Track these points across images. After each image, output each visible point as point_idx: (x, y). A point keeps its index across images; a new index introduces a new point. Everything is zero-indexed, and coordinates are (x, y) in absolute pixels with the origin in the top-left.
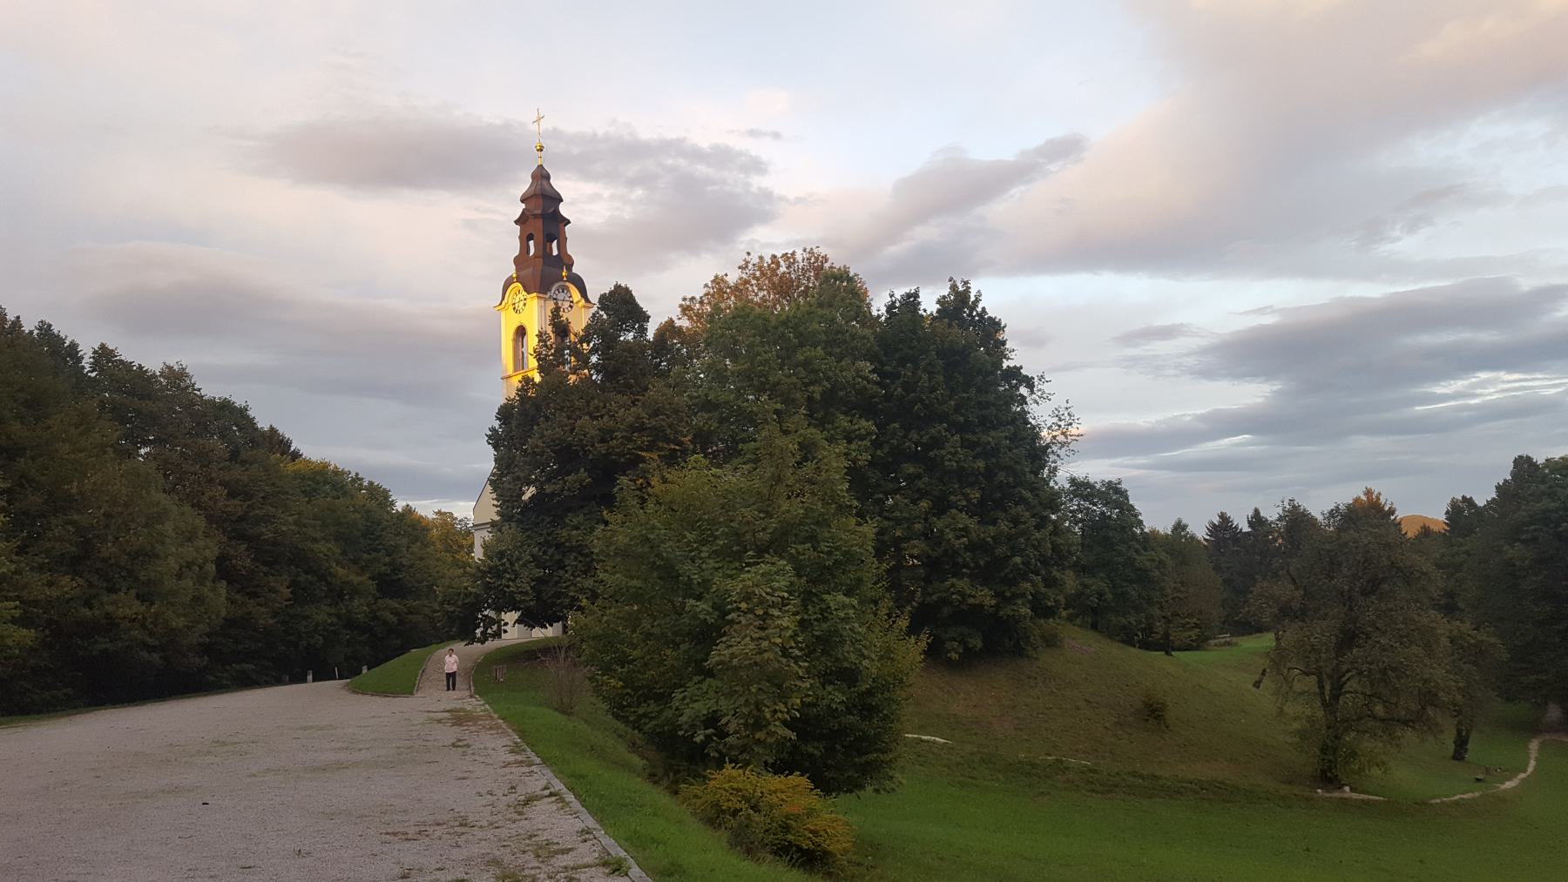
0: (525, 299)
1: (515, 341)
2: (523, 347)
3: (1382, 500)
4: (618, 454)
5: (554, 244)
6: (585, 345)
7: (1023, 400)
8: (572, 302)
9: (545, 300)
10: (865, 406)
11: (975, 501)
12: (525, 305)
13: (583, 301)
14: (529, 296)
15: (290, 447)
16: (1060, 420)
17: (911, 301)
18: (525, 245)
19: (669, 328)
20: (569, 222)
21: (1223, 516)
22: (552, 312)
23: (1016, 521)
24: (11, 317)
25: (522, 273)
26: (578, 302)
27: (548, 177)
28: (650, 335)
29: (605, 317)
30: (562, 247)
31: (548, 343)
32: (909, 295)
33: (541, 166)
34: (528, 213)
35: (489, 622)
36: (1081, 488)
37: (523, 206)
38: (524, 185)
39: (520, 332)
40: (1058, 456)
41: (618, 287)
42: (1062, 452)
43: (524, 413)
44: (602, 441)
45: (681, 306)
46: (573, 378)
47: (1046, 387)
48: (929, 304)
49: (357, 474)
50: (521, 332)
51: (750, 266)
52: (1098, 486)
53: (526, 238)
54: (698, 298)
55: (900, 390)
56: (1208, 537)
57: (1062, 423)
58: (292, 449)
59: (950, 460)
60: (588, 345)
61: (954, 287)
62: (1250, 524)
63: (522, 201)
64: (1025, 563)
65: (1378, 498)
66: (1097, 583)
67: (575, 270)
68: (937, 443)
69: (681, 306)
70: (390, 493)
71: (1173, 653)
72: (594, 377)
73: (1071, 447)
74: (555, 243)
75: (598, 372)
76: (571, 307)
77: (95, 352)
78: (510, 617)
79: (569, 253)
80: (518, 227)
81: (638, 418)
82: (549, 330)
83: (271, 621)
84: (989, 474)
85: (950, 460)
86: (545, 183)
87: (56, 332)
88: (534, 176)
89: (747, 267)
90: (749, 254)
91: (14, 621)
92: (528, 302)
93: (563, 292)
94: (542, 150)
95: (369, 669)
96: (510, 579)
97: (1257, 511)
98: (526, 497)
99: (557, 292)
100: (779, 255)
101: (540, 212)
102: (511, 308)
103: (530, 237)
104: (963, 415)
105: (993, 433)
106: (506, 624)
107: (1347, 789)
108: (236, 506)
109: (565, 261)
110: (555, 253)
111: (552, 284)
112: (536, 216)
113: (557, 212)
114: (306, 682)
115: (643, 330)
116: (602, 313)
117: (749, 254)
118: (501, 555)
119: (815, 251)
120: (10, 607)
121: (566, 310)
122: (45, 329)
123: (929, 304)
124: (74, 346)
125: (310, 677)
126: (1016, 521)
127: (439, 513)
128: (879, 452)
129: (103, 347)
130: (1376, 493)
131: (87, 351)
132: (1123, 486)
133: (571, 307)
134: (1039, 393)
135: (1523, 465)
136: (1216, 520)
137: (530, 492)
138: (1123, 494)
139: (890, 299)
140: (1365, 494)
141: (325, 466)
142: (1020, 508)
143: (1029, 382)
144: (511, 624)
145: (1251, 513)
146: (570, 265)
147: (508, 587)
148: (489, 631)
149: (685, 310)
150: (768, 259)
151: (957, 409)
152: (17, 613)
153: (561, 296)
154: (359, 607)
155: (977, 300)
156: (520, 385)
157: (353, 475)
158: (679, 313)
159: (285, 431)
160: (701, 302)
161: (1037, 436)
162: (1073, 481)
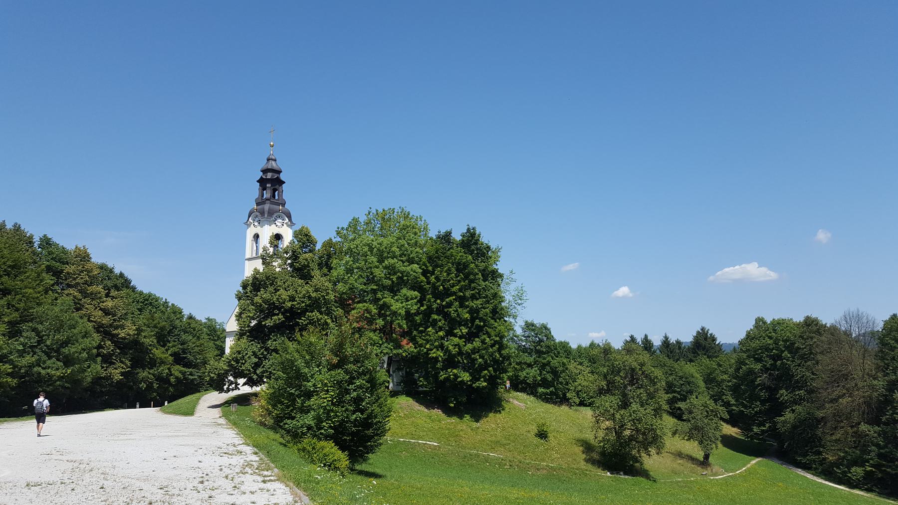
0: (260, 221)
3: (710, 332)
4: (296, 308)
6: (285, 255)
7: (499, 285)
8: (283, 223)
9: (270, 221)
10: (416, 286)
15: (130, 283)
16: (518, 293)
17: (448, 235)
18: (261, 194)
19: (329, 244)
20: (285, 183)
21: (632, 337)
22: (270, 237)
23: (483, 342)
24: (9, 226)
25: (259, 207)
26: (286, 223)
29: (297, 243)
30: (280, 195)
31: (268, 252)
34: (264, 177)
35: (231, 383)
36: (529, 326)
37: (262, 173)
38: (263, 164)
39: (256, 236)
40: (518, 310)
42: (519, 307)
43: (253, 284)
44: (290, 301)
45: (337, 231)
46: (278, 270)
48: (457, 236)
49: (166, 300)
50: (256, 237)
51: (371, 214)
54: (345, 228)
55: (433, 279)
57: (519, 294)
58: (132, 284)
59: (454, 313)
60: (287, 255)
61: (468, 229)
62: (643, 343)
64: (486, 362)
65: (708, 332)
66: (532, 374)
67: (286, 206)
68: (449, 305)
69: (337, 231)
70: (183, 311)
72: (289, 269)
73: (523, 305)
74: (277, 192)
75: (291, 267)
77: (41, 239)
78: (241, 381)
79: (284, 198)
80: (259, 184)
81: (308, 292)
82: (268, 245)
83: (121, 377)
84: (473, 320)
85: (454, 313)
86: (273, 162)
87: (22, 228)
88: (268, 160)
89: (369, 214)
90: (370, 208)
91: (8, 374)
92: (261, 222)
95: (168, 403)
96: (242, 363)
97: (646, 335)
98: (252, 325)
99: (276, 218)
100: (386, 209)
101: (270, 177)
102: (252, 225)
103: (264, 189)
104: (463, 293)
105: (475, 302)
106: (239, 384)
107: (622, 473)
108: (106, 320)
110: (277, 198)
112: (268, 180)
113: (278, 178)
114: (135, 407)
116: (295, 240)
117: (370, 208)
118: (239, 352)
119: (404, 209)
120: (8, 368)
122: (17, 228)
123: (457, 236)
124: (31, 237)
125: (138, 406)
126: (483, 342)
127: (208, 319)
128: (422, 308)
129: (45, 236)
130: (707, 329)
131: (36, 240)
132: (549, 326)
133: (283, 225)
134: (510, 279)
135: (760, 322)
136: (628, 339)
137: (253, 323)
138: (549, 330)
139: (438, 234)
140: (702, 330)
141: (150, 295)
142: (485, 336)
143: (501, 276)
144: (241, 385)
145: (643, 337)
146: (283, 205)
147: (241, 367)
148: (230, 387)
149: (338, 233)
150: (380, 210)
151: (460, 290)
152: (10, 371)
154: (164, 370)
155: (479, 236)
156: (253, 273)
157: (164, 300)
158: (335, 233)
159: (128, 274)
160: (347, 229)
161: (502, 300)
162: (526, 322)
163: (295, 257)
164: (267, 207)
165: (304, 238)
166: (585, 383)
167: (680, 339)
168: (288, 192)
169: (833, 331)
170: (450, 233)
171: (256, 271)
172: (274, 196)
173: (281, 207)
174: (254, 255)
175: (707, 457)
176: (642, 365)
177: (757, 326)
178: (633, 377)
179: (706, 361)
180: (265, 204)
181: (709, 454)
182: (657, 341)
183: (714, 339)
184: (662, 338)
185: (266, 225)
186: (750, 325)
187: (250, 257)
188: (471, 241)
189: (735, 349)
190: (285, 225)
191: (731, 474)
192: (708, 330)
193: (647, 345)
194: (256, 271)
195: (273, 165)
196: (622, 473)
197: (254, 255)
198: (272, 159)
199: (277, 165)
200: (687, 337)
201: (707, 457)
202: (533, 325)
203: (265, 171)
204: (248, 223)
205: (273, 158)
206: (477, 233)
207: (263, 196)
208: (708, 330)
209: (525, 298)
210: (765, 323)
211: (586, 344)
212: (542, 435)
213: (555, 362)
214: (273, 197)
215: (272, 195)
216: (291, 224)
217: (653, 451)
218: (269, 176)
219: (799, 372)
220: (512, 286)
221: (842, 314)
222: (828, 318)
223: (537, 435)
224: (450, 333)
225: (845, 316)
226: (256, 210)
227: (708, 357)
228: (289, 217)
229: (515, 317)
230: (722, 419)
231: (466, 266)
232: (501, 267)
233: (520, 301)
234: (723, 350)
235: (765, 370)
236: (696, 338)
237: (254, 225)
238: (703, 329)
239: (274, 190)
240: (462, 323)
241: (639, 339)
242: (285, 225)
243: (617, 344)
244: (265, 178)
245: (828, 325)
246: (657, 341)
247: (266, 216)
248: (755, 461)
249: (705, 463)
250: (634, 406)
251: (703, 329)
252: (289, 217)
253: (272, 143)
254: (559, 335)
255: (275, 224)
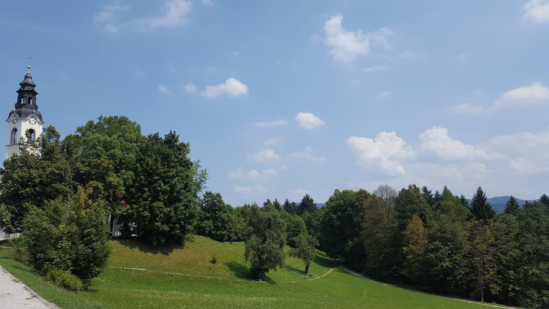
0: (18, 119)
1: (12, 133)
2: (15, 135)
3: (310, 198)
5: (31, 101)
8: (36, 121)
9: (25, 120)
11: (166, 199)
12: (17, 121)
13: (40, 122)
14: (19, 119)
20: (37, 94)
21: (268, 200)
27: (31, 78)
28: (61, 139)
32: (156, 134)
33: (29, 74)
34: (22, 89)
36: (208, 194)
37: (21, 86)
38: (22, 80)
39: (15, 129)
41: (51, 126)
47: (200, 164)
48: (162, 136)
52: (214, 194)
53: (20, 98)
56: (263, 206)
61: (171, 132)
63: (20, 85)
65: (309, 197)
67: (38, 110)
68: (156, 181)
71: (233, 243)
76: (35, 123)
79: (36, 104)
80: (18, 93)
86: (30, 80)
88: (26, 77)
93: (33, 118)
94: (30, 68)
97: (276, 199)
99: (30, 118)
102: (12, 121)
103: (23, 97)
107: (261, 280)
109: (36, 108)
110: (31, 104)
111: (29, 115)
115: (58, 138)
121: (33, 124)
123: (162, 136)
130: (309, 195)
135: (336, 190)
136: (266, 201)
140: (306, 196)
153: (32, 119)
163: (44, 144)
164: (23, 110)
165: (51, 132)
166: (241, 227)
167: (294, 201)
168: (39, 100)
169: (374, 196)
170: (158, 134)
171: (14, 155)
172: (29, 103)
173: (34, 111)
174: (13, 144)
175: (307, 268)
176: (275, 217)
177: (335, 194)
178: (269, 224)
179: (307, 214)
180: (22, 108)
181: (308, 267)
182: (282, 203)
183: (312, 201)
184: (285, 201)
185: (23, 122)
186: (331, 194)
187: (9, 144)
188: (171, 140)
189: (323, 207)
190: (36, 123)
191: (320, 277)
192: (310, 196)
193: (277, 205)
194: (14, 155)
195: (29, 81)
196: (261, 280)
197: (13, 144)
198: (28, 77)
199: (32, 80)
200: (298, 200)
201: (307, 268)
202: (210, 193)
203: (23, 85)
204: (9, 119)
205: (29, 76)
206: (177, 135)
207: (21, 101)
208: (310, 196)
209: (207, 177)
210: (339, 192)
211: (242, 205)
212: (214, 262)
213: (224, 216)
214: (28, 103)
215: (28, 102)
216: (42, 122)
217: (278, 267)
218: (26, 89)
219: (356, 219)
220: (199, 169)
221: (378, 187)
222: (371, 189)
223: (211, 261)
224: (156, 198)
225: (379, 189)
226: (15, 111)
227: (310, 211)
228: (40, 118)
229: (199, 188)
230: (316, 247)
231: (168, 156)
232: (191, 157)
233: (203, 179)
234: (317, 207)
235: (338, 218)
236: (303, 200)
237: (13, 122)
238: (307, 196)
239: (30, 99)
240: (164, 192)
241: (272, 201)
242: (36, 123)
243: (261, 205)
244: (23, 89)
245: (371, 194)
246: (282, 203)
247: (22, 116)
248: (332, 269)
249: (306, 272)
250: (269, 240)
251: (307, 196)
252: (40, 118)
253: (29, 66)
254: (227, 200)
255: (29, 122)
